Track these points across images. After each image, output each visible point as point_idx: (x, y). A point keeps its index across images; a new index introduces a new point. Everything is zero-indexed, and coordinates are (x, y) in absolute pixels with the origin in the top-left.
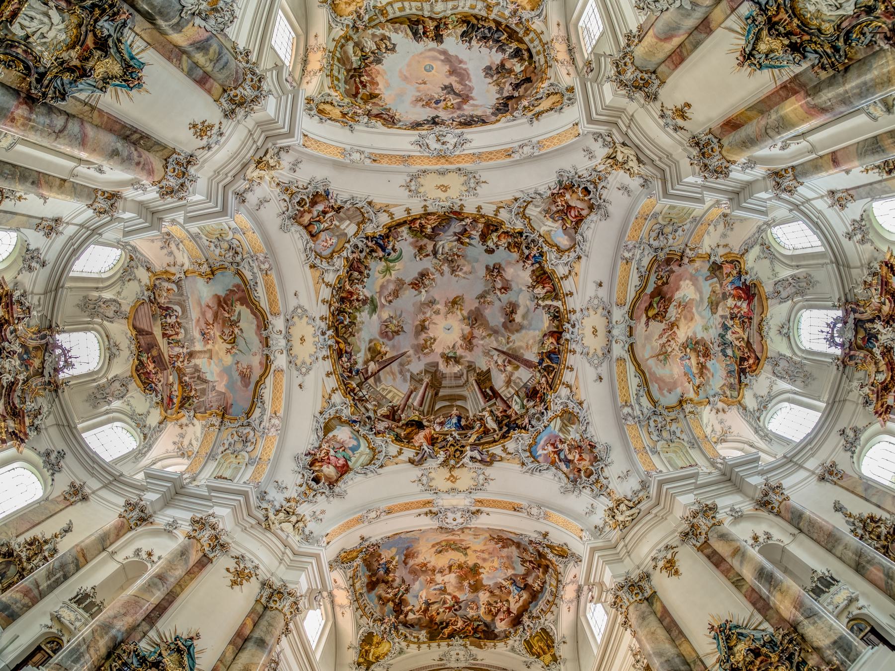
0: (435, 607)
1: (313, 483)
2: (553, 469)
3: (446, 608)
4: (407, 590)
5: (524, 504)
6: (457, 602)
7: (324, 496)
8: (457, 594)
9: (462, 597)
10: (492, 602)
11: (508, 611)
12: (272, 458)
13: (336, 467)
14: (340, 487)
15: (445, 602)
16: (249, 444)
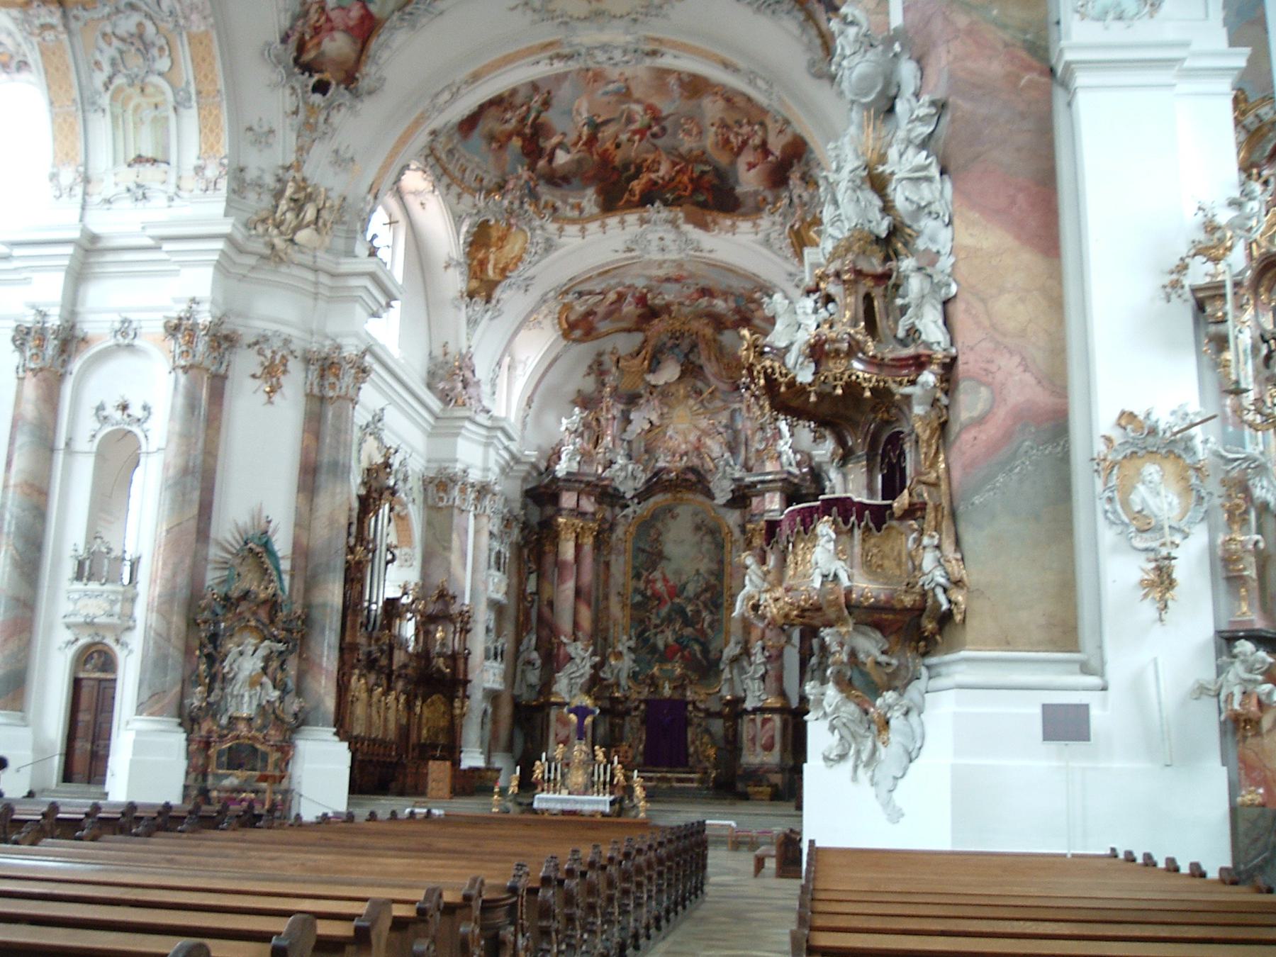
0: (608, 131)
1: (317, 98)
2: (801, 16)
3: (635, 132)
4: (546, 104)
5: (742, 64)
6: (656, 118)
7: (343, 110)
8: (657, 101)
9: (666, 107)
10: (730, 122)
11: (764, 148)
12: (221, 84)
13: (348, 30)
14: (369, 72)
15: (630, 120)
16: (155, 52)
